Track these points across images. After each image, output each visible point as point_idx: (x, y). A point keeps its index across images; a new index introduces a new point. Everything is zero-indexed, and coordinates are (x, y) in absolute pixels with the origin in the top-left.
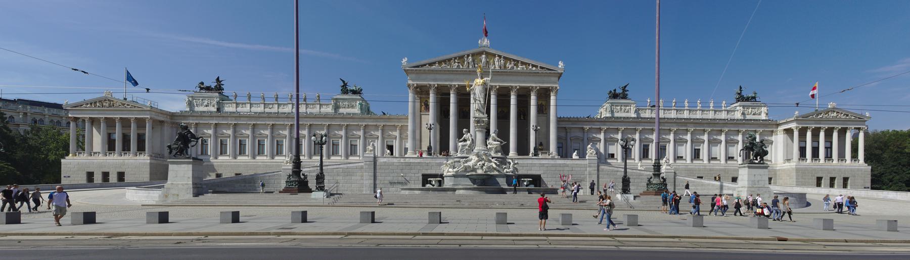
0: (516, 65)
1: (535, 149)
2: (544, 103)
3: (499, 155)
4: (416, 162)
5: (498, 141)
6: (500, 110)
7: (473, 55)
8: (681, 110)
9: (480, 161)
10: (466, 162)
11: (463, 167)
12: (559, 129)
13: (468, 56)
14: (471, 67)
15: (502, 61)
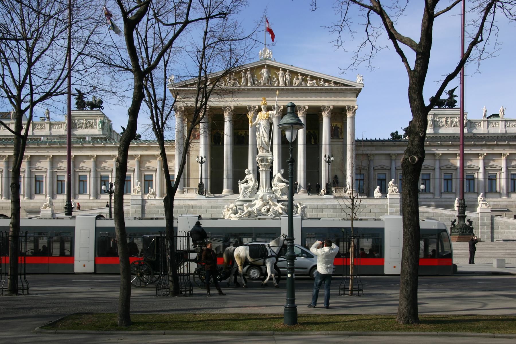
0: (305, 80)
1: (327, 185)
2: (339, 125)
3: (285, 197)
9: (265, 205)
10: (251, 206)
11: (247, 213)
12: (357, 156)
14: (249, 84)
15: (287, 76)
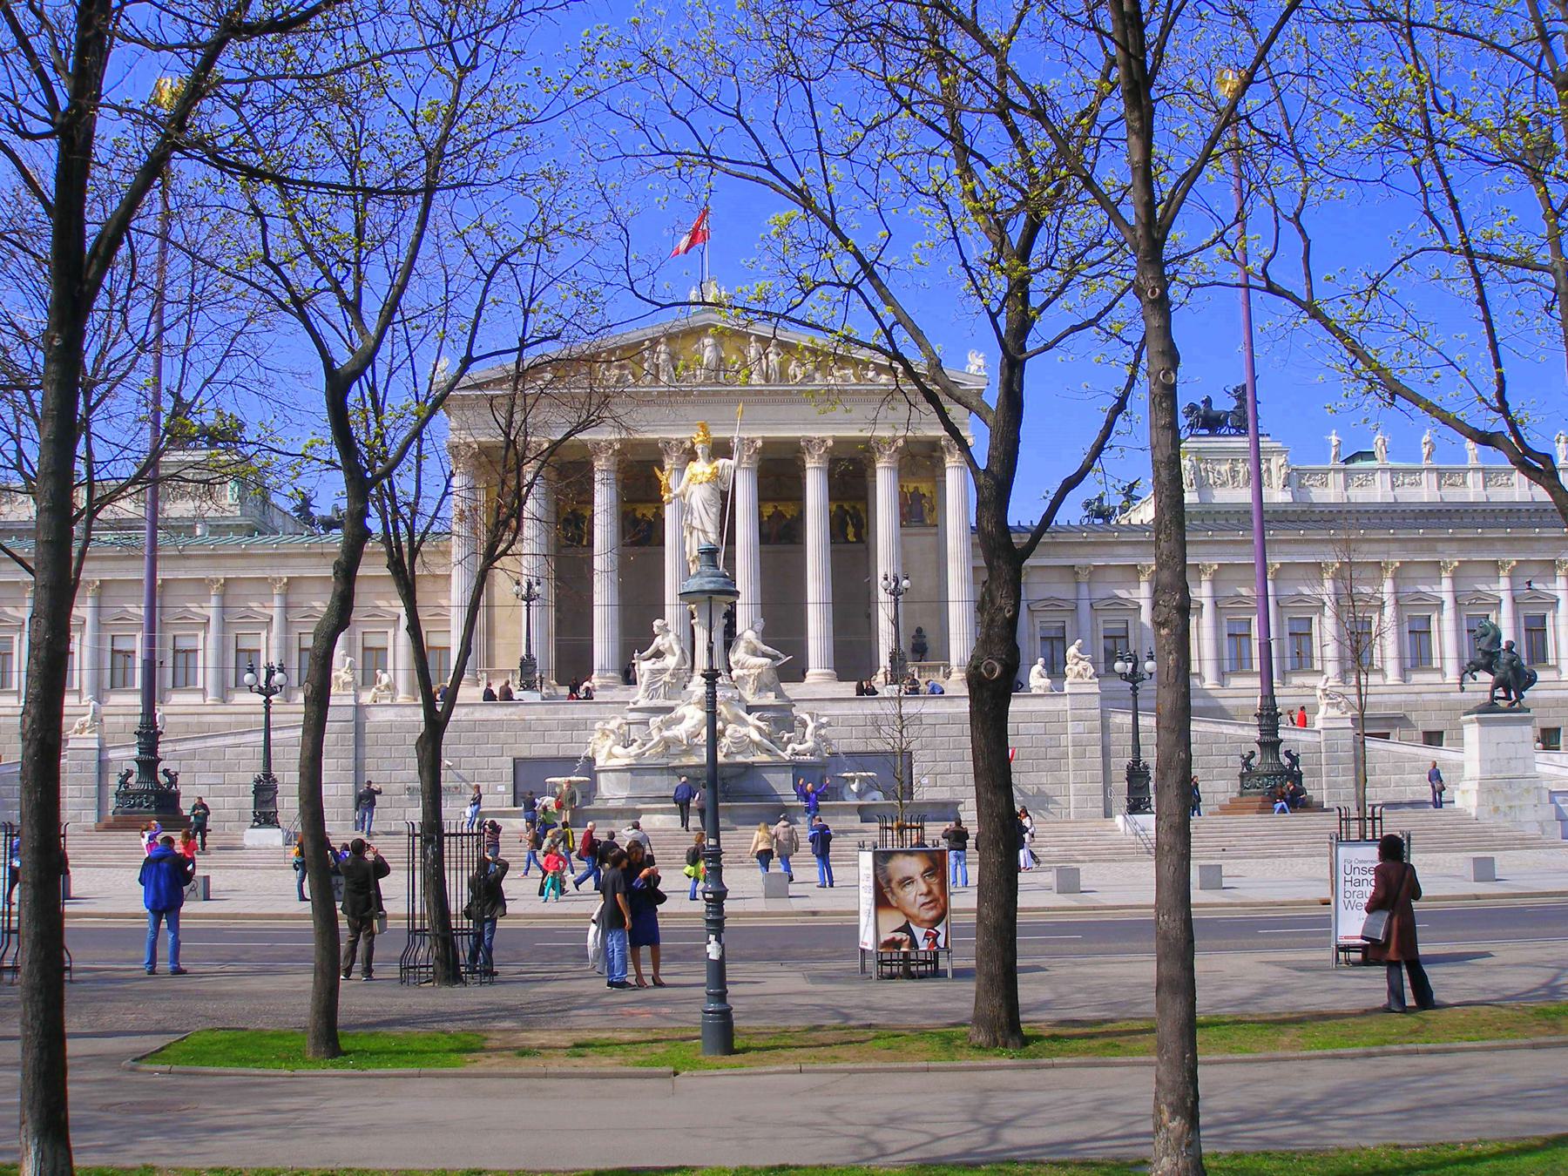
1: (895, 657)
2: (924, 488)
4: (495, 718)
5: (765, 655)
6: (769, 510)
7: (670, 337)
8: (1453, 472)
10: (668, 725)
11: (659, 742)
13: (655, 342)
14: (664, 378)
15: (771, 357)
